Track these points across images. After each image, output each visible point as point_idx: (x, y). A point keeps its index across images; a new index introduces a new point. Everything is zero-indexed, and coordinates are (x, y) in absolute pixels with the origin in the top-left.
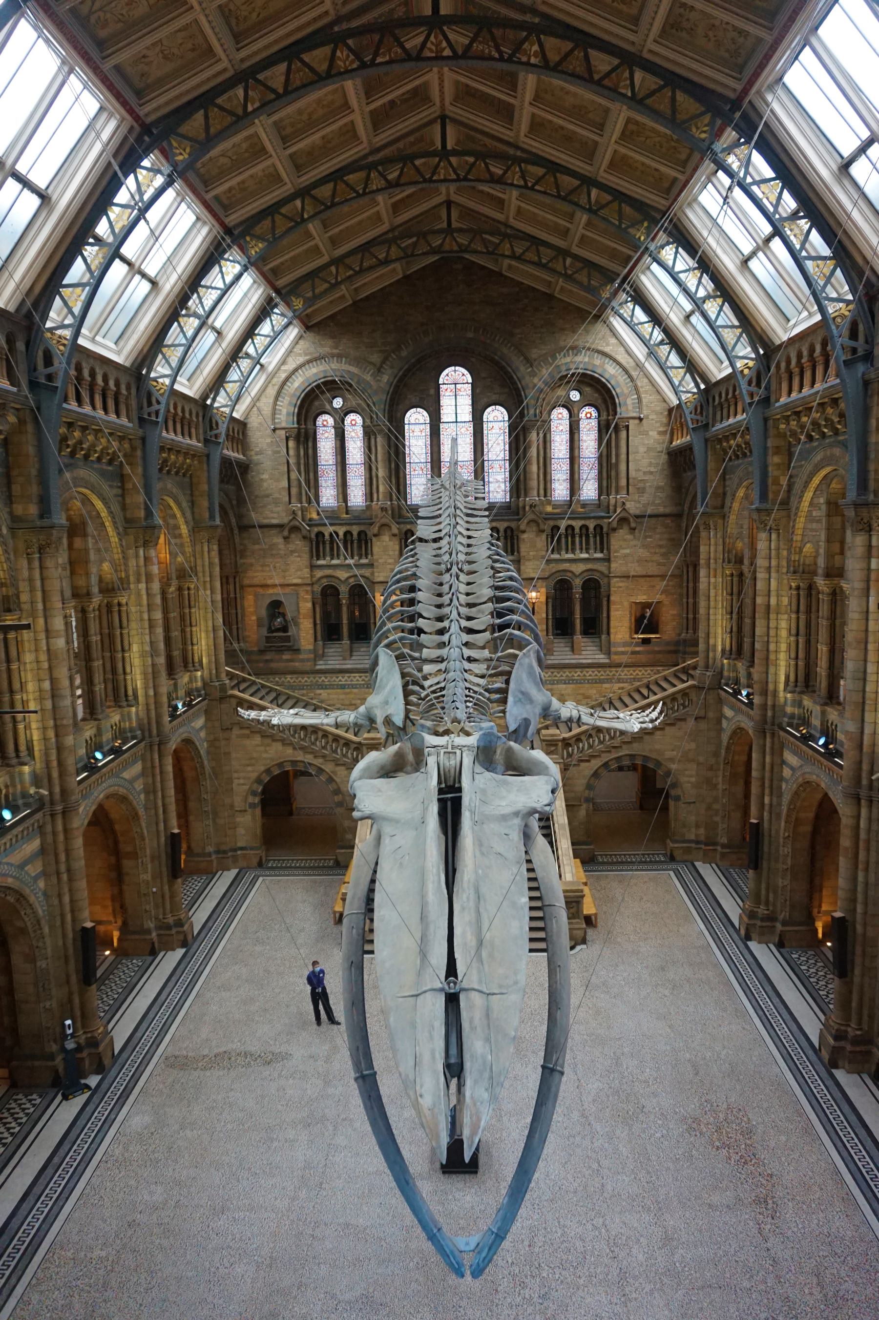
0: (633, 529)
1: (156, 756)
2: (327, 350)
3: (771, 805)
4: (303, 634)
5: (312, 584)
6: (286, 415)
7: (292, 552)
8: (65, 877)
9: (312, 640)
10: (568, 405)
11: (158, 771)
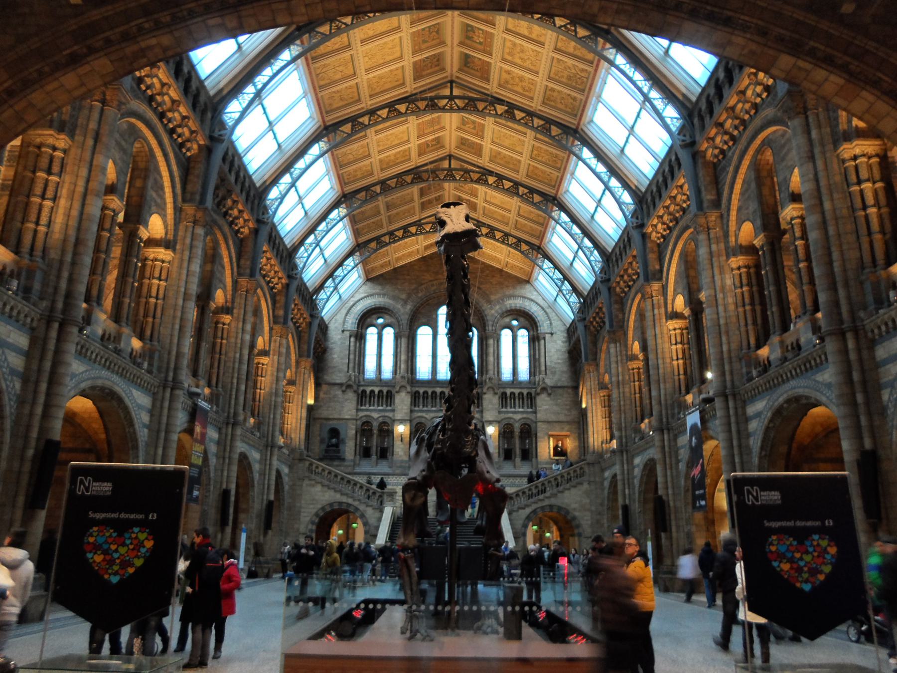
0: (549, 395)
1: (269, 453)
2: (378, 291)
3: (629, 494)
4: (347, 449)
5: (356, 420)
6: (351, 323)
7: (347, 400)
8: (227, 461)
9: (353, 453)
10: (510, 327)
11: (268, 462)
